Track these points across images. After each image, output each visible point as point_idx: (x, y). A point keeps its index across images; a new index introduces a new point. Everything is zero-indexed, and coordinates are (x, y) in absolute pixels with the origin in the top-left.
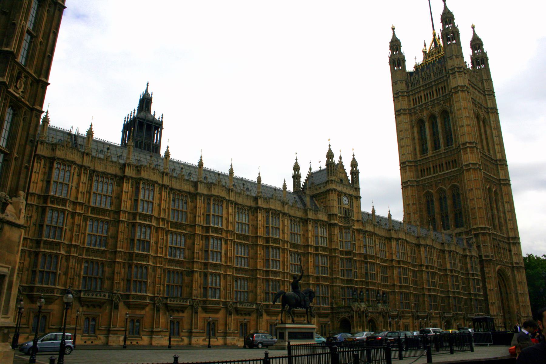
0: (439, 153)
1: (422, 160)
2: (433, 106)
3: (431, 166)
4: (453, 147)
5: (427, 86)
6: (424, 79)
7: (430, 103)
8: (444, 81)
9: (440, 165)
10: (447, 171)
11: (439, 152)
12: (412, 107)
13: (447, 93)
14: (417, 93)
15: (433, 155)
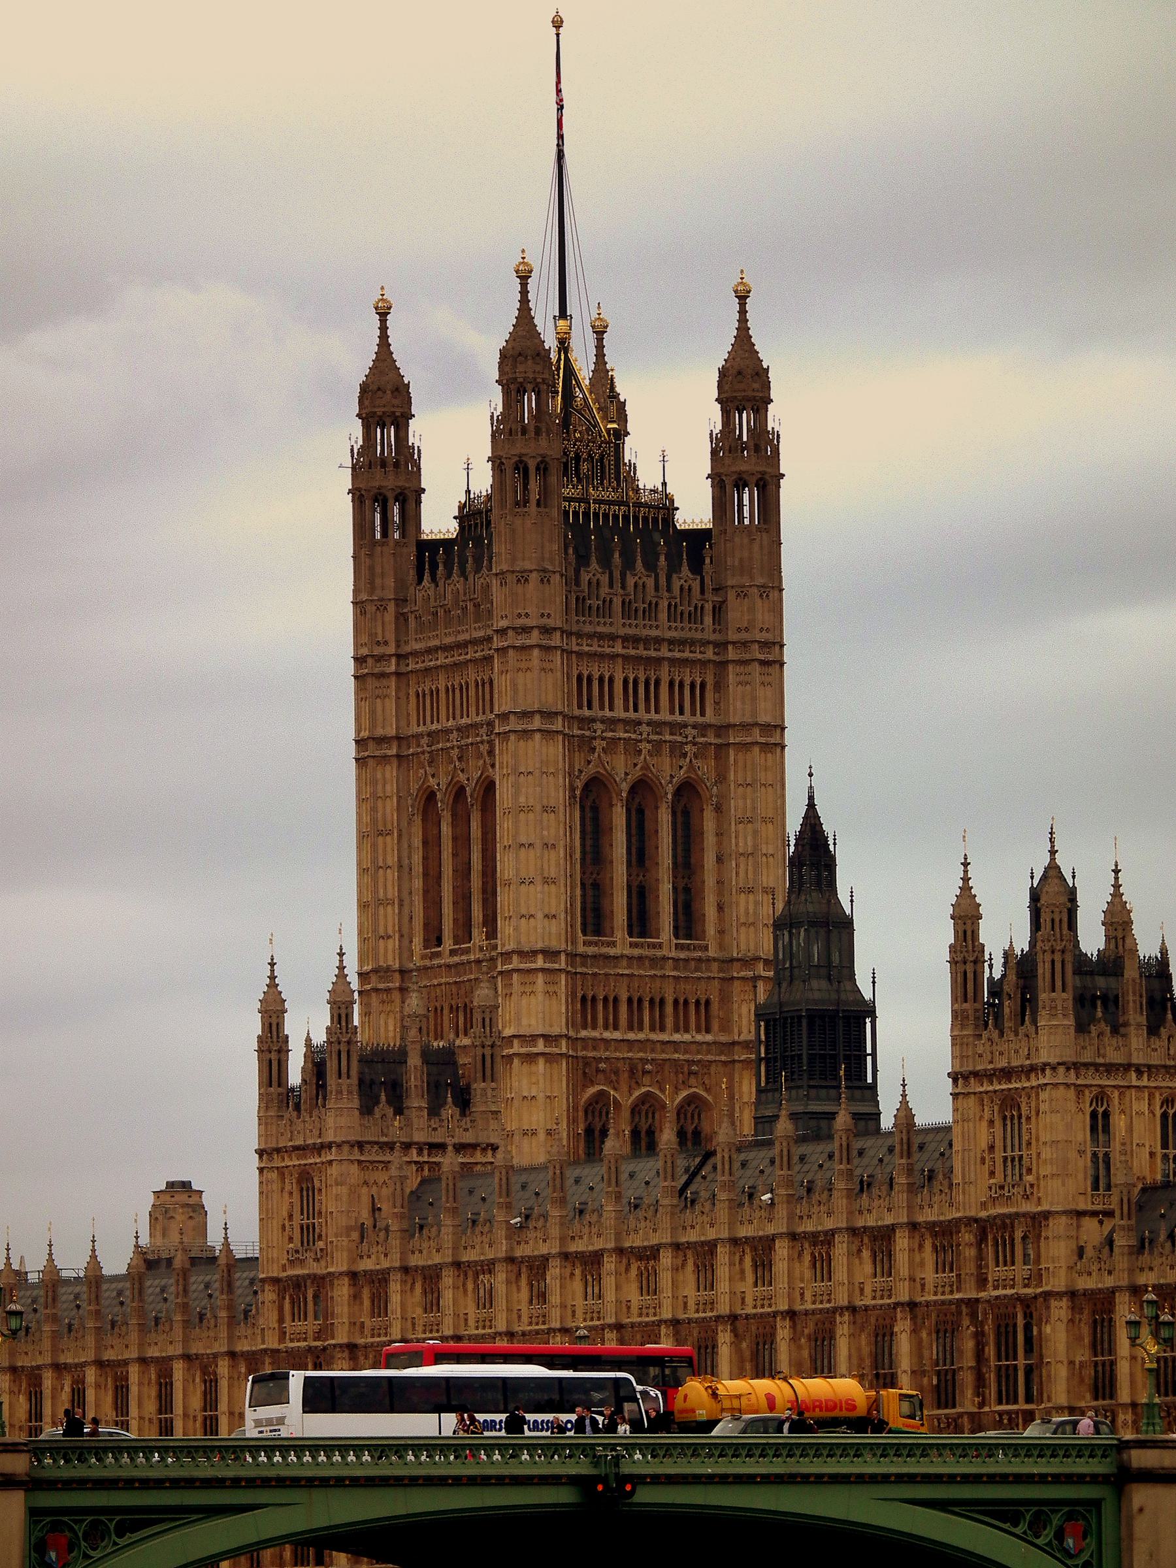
0: (659, 953)
1: (594, 957)
2: (657, 746)
3: (624, 997)
4: (706, 948)
5: (641, 652)
6: (628, 610)
7: (645, 728)
8: (704, 663)
9: (652, 1001)
10: (677, 1037)
11: (654, 946)
12: (577, 712)
13: (710, 717)
14: (602, 656)
15: (637, 952)
